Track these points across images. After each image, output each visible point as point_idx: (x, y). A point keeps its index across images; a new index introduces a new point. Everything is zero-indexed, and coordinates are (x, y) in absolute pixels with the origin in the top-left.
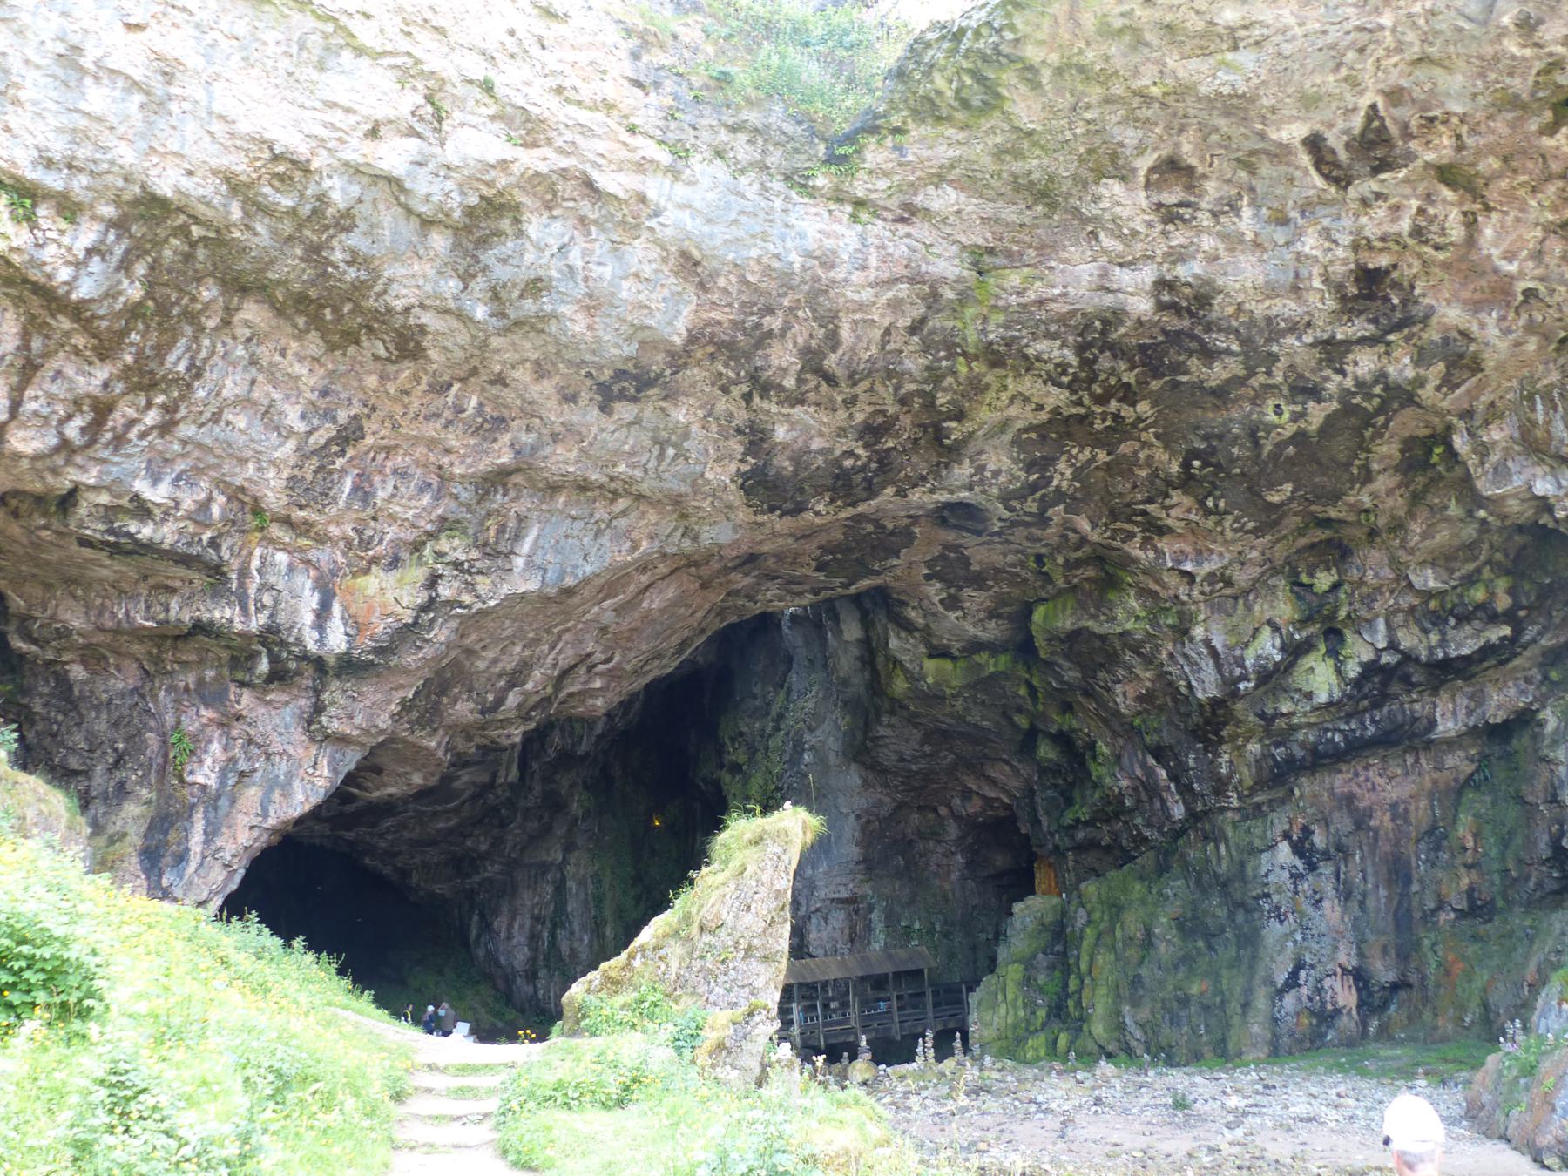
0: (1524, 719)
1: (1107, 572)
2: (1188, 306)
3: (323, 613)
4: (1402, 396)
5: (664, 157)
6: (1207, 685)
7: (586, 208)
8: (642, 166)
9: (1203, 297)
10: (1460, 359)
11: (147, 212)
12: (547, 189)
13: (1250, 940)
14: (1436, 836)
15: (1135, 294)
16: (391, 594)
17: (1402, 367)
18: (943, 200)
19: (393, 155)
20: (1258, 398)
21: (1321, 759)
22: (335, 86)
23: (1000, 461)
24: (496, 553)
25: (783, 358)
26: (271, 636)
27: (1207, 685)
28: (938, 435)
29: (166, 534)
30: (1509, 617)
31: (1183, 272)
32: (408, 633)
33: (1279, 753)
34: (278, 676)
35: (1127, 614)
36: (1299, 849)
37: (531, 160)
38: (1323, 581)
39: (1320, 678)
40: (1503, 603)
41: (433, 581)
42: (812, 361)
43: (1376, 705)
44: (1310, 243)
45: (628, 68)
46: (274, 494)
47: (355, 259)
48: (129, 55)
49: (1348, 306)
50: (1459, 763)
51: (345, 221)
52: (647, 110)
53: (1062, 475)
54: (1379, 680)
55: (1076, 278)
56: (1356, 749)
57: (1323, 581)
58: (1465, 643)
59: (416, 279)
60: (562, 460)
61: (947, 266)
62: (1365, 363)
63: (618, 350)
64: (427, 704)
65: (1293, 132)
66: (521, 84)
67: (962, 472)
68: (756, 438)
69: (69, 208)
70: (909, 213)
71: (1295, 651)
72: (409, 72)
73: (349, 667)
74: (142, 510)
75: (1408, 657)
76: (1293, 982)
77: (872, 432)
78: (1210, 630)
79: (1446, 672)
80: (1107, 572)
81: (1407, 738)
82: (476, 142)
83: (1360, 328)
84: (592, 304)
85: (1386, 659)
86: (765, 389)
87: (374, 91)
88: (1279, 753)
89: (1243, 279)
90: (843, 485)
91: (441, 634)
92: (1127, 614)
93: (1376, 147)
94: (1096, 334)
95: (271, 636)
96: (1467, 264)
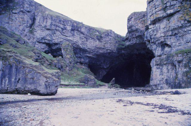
11: (97, 55)
17: (150, 55)
19: (106, 52)
37: (111, 51)
46: (103, 62)
66: (110, 49)
69: (95, 55)
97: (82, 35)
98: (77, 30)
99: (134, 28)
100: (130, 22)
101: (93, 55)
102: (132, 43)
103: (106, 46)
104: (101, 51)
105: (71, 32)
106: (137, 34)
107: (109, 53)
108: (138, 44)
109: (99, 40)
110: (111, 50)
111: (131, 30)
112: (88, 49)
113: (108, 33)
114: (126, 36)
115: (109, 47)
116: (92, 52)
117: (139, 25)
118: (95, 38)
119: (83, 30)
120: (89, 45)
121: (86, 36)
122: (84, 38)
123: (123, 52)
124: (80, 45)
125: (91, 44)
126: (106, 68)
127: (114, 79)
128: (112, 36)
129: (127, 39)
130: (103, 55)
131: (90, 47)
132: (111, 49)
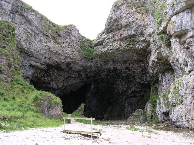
0: (143, 95)
1: (114, 83)
2: (115, 69)
3: (56, 86)
4: (131, 74)
5: (80, 60)
6: (121, 92)
7: (75, 63)
8: (79, 60)
9: (116, 68)
10: (134, 73)
11: (48, 65)
12: (73, 62)
13: (124, 111)
14: (137, 103)
15: (112, 68)
16: (61, 85)
17: (130, 72)
18: (99, 62)
19: (63, 61)
20: (122, 73)
21: (130, 97)
22: (60, 57)
23: (104, 76)
24: (68, 82)
25: (88, 70)
26: (53, 87)
27: (121, 92)
28: (99, 75)
29: (47, 81)
30: (141, 88)
31: (115, 67)
32: (61, 87)
33: (127, 96)
34: (53, 90)
35: (115, 86)
36: (128, 104)
38: (129, 84)
39: (130, 92)
40: (141, 87)
41: (64, 84)
42: (90, 71)
43: (133, 93)
44: (123, 66)
45: (78, 54)
47: (60, 66)
48: (48, 56)
49: (126, 69)
50: (140, 98)
51: (60, 64)
52: (79, 57)
53: (109, 77)
54: (133, 92)
55: (108, 66)
56: (132, 97)
57: (129, 84)
58: (138, 90)
59: (64, 67)
60: (73, 76)
61: (99, 66)
62: (128, 72)
63: (77, 70)
64: (62, 92)
65: (121, 60)
66: (71, 56)
67: (102, 76)
68: (86, 75)
69: (44, 65)
70: (96, 63)
71: (127, 90)
72: (64, 56)
73: (57, 89)
74: (45, 80)
75: (135, 90)
76: (126, 114)
77: (95, 74)
78: (121, 88)
79: (138, 92)
80: (114, 83)
81: (135, 96)
82: (68, 60)
83: (127, 70)
84: (75, 68)
85: (134, 90)
86: (87, 72)
87: (62, 57)
88: (127, 96)
89: (119, 67)
90: (93, 77)
91: (64, 87)
92: (115, 86)
93: (126, 61)
94: (109, 70)
95: (53, 87)
96: (133, 67)
97: (28, 25)
98: (22, 15)
99: (123, 22)
100: (119, 12)
101: (42, 64)
102: (111, 50)
103: (65, 51)
104: (56, 59)
105: (9, 15)
106: (125, 34)
107: (68, 64)
108: (122, 50)
109: (54, 38)
110: (72, 59)
111: (113, 26)
112: (35, 53)
113: (69, 30)
114: (99, 38)
115: (70, 53)
116: (41, 59)
117: (136, 17)
118: (49, 36)
119: (30, 17)
120: (38, 45)
121: (34, 28)
122: (30, 31)
123: (89, 64)
124: (23, 43)
125: (39, 45)
126: (57, 88)
127: (83, 105)
128: (75, 37)
129: (100, 44)
130: (57, 67)
131: (38, 49)
132: (73, 57)
